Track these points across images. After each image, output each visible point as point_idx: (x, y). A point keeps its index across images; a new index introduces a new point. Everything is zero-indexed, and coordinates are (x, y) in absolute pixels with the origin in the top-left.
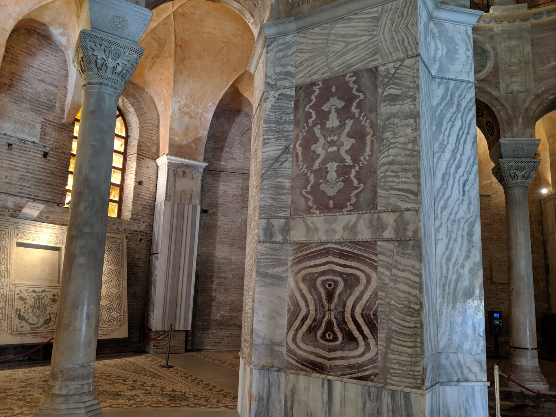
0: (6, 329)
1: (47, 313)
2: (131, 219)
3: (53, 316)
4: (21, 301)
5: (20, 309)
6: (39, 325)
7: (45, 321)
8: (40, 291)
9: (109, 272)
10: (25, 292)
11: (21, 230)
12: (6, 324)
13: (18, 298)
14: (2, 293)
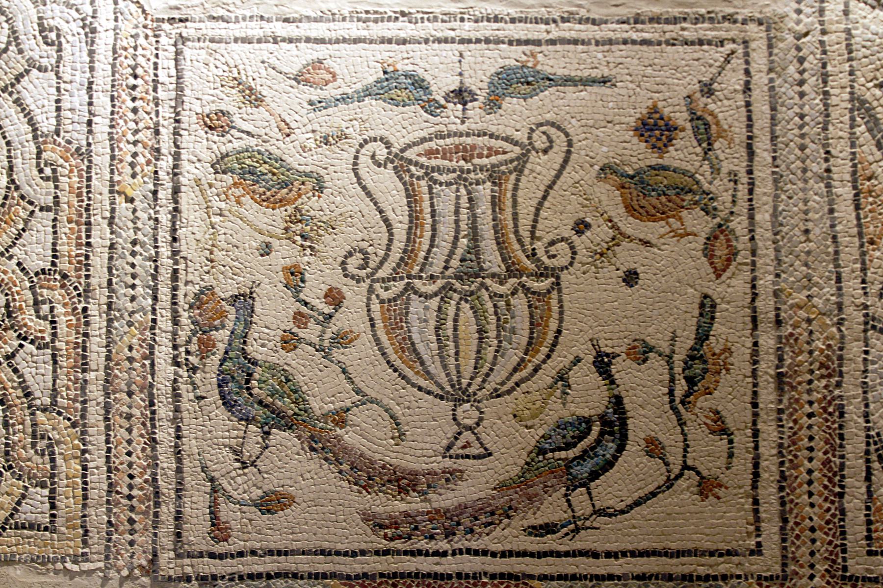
0: (98, 516)
4: (251, 209)
7: (542, 452)
12: (97, 460)
13: (220, 165)
14: (47, 125)
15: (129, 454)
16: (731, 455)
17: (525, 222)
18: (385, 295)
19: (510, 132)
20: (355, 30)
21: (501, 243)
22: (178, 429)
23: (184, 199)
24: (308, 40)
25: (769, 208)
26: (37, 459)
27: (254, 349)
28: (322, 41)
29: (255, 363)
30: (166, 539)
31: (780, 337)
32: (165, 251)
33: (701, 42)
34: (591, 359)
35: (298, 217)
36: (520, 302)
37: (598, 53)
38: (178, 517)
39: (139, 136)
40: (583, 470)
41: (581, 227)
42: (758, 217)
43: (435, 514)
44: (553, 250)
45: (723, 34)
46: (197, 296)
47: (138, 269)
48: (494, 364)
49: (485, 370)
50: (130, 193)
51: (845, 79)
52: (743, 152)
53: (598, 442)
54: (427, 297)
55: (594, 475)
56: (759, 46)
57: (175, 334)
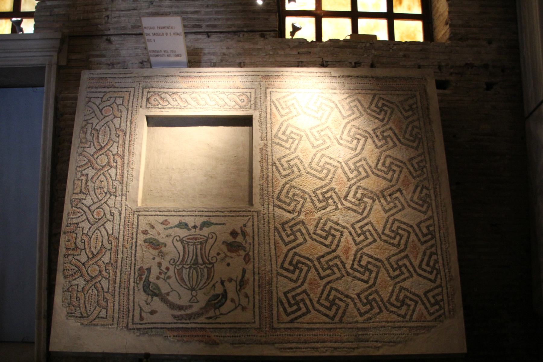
0: (116, 315)
1: (217, 278)
2: (450, 39)
3: (231, 288)
4: (151, 250)
5: (149, 270)
6: (196, 308)
7: (209, 301)
8: (198, 224)
9: (390, 168)
10: (160, 228)
11: (156, 90)
12: (117, 304)
13: (145, 241)
14: (110, 232)
15: (123, 302)
16: (249, 302)
17: (207, 253)
18: (178, 268)
19: (204, 234)
20: (174, 213)
21: (202, 257)
22: (134, 297)
23: (138, 248)
24: (164, 216)
25: (257, 250)
26: (104, 303)
27: (151, 279)
28: (167, 216)
29: (151, 282)
30: (130, 320)
31: (259, 277)
32: (133, 259)
33: (244, 216)
34: (219, 281)
35: (161, 252)
36: (205, 270)
37: (223, 218)
38: (133, 315)
39: (129, 235)
40: (217, 305)
41: (218, 254)
42: (255, 252)
43: (187, 315)
44: (213, 259)
45: (248, 214)
46: (139, 268)
47: (127, 263)
48: (200, 282)
49: (198, 284)
50: (126, 247)
51: (273, 223)
52: (252, 239)
53: (221, 299)
54: (187, 269)
55: (220, 306)
56: (256, 217)
57: (134, 276)
